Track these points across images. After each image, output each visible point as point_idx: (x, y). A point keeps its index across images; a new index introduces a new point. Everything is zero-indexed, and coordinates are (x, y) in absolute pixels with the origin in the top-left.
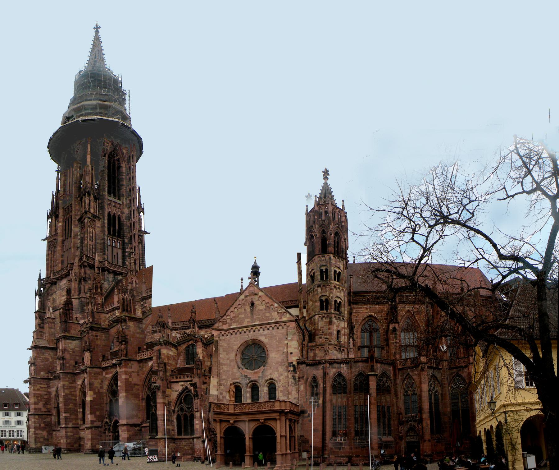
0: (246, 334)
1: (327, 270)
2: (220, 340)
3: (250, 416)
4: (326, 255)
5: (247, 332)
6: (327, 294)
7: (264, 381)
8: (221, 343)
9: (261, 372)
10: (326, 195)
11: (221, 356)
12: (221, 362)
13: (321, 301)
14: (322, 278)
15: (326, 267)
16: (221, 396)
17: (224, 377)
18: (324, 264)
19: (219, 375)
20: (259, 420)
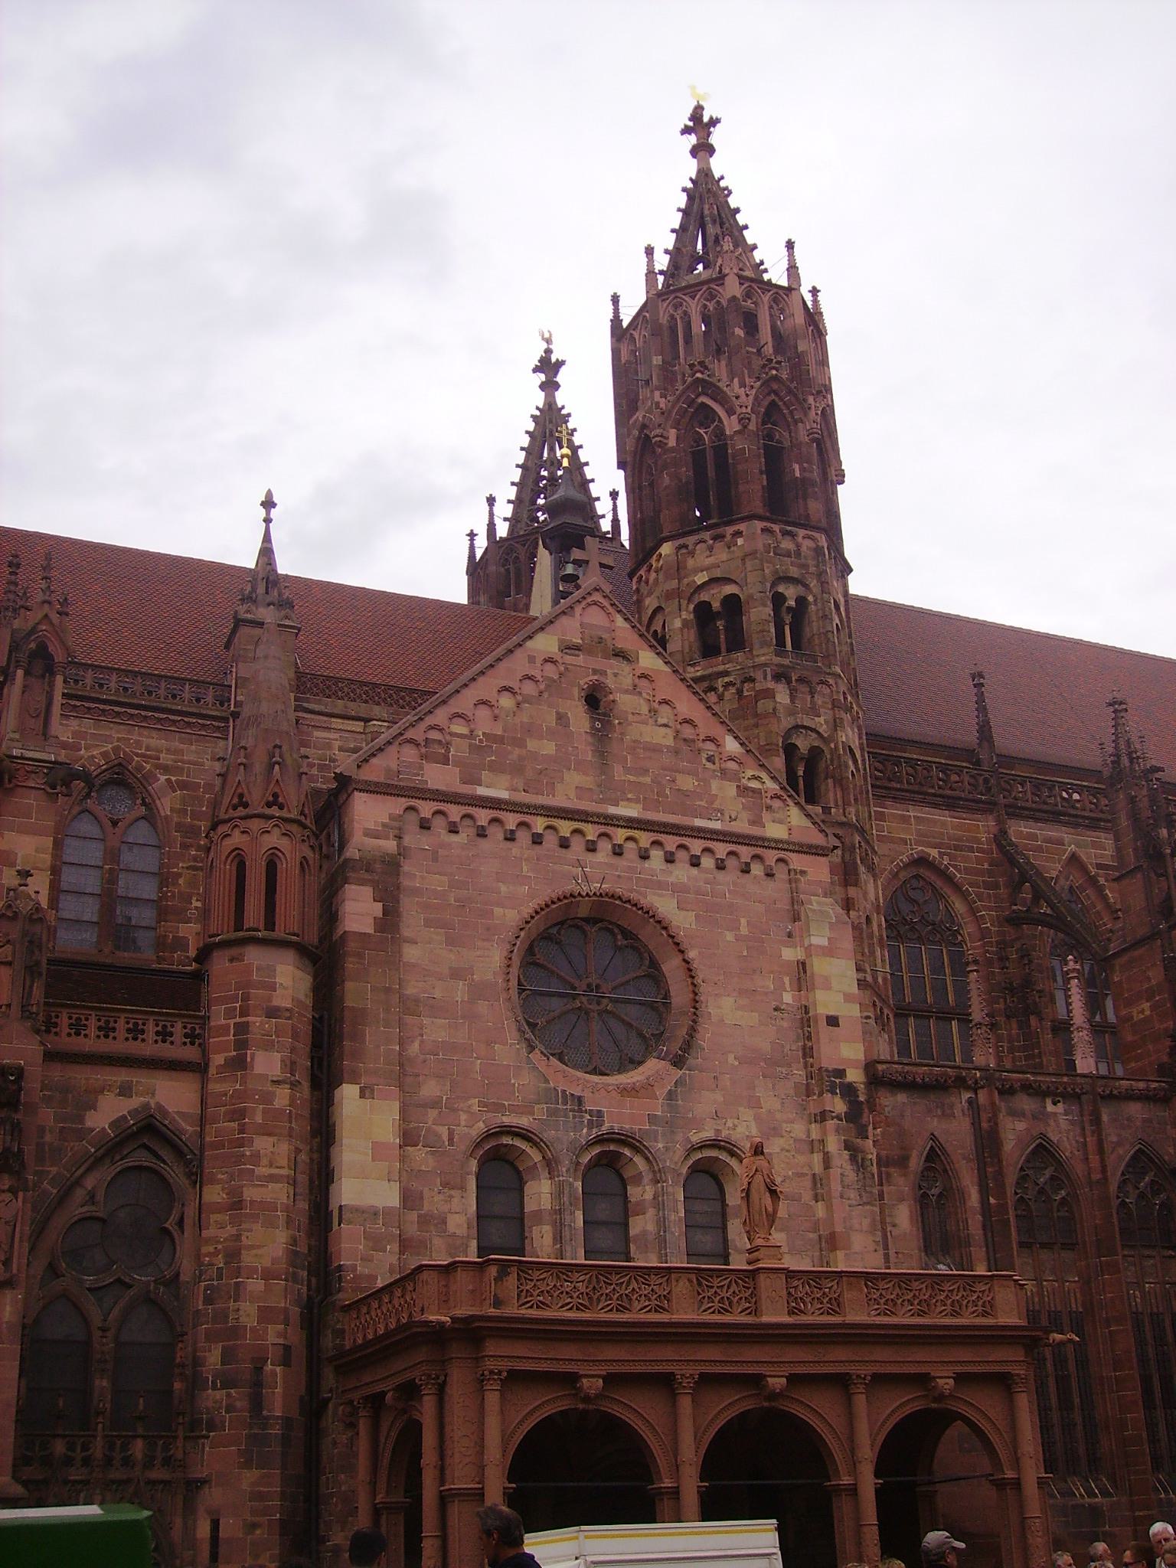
0: (570, 855)
1: (801, 601)
2: (403, 852)
3: (712, 1352)
4: (801, 532)
5: (577, 845)
6: (821, 722)
7: (680, 1150)
8: (414, 875)
9: (661, 1092)
10: (708, 211)
11: (411, 953)
12: (410, 991)
13: (790, 750)
14: (780, 642)
15: (800, 590)
16: (413, 1216)
17: (430, 1089)
18: (794, 572)
19: (403, 1076)
20: (756, 1381)
